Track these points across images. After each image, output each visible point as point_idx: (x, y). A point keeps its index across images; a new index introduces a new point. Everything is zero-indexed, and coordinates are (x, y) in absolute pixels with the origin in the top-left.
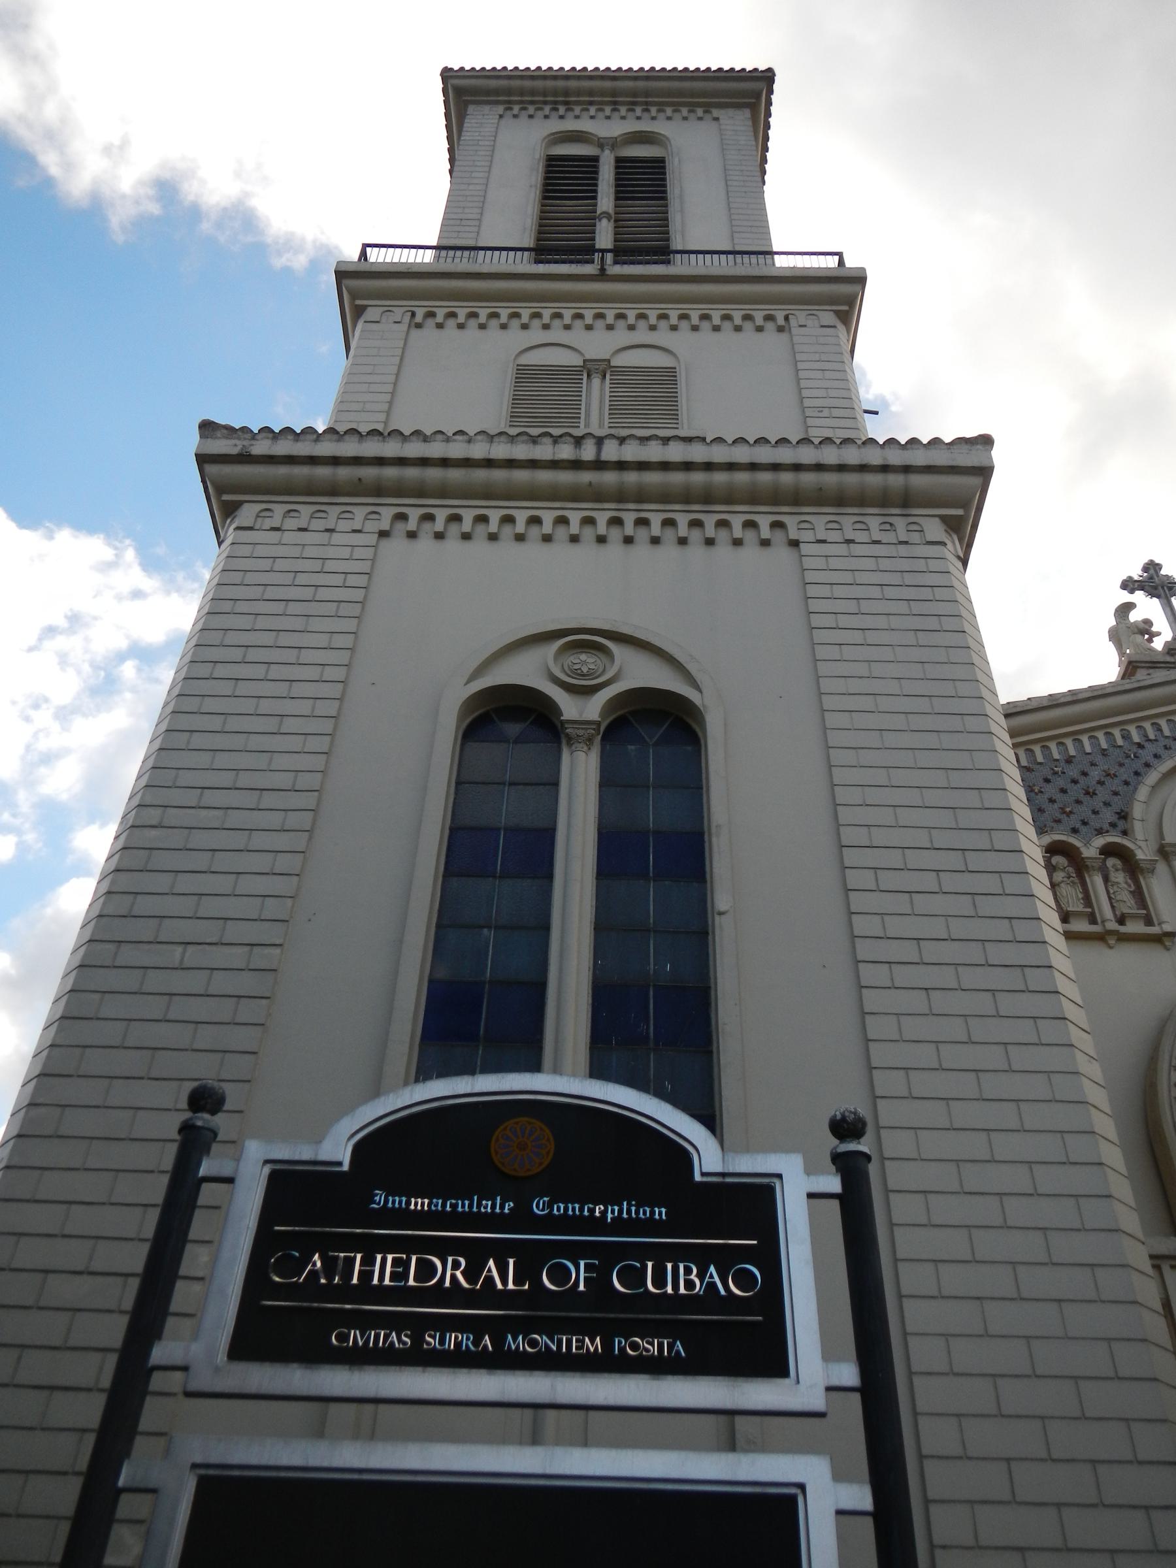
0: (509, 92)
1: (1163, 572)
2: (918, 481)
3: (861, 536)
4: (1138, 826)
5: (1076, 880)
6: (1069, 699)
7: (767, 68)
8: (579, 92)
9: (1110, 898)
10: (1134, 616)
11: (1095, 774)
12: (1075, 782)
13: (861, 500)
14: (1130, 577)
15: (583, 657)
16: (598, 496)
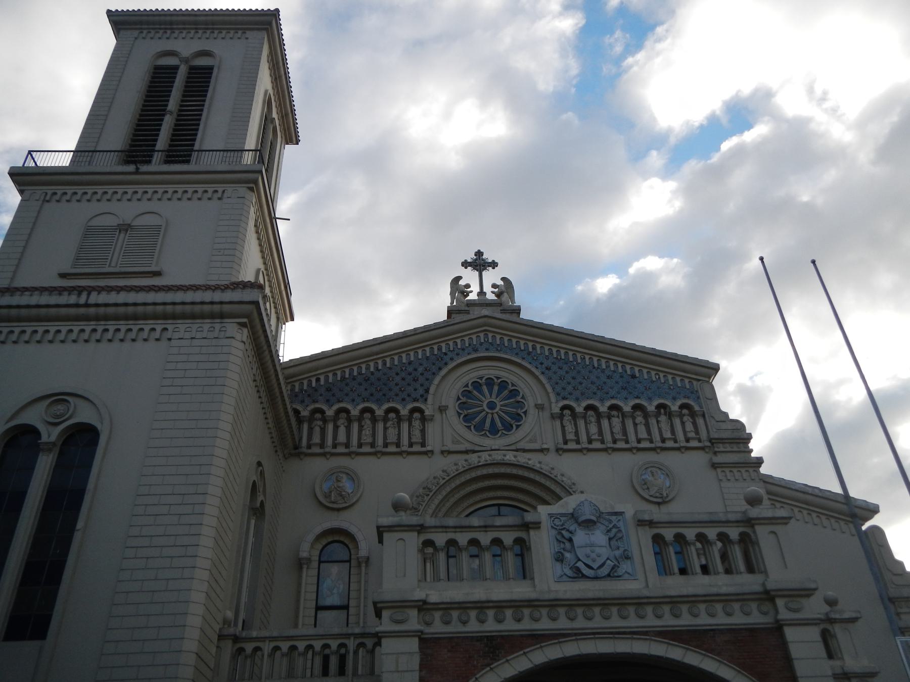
0: (141, 23)
1: (484, 257)
2: (226, 308)
3: (199, 335)
4: (430, 398)
5: (396, 425)
6: (413, 333)
7: (274, 8)
8: (178, 23)
9: (409, 433)
10: (462, 283)
11: (421, 369)
12: (410, 374)
13: (202, 316)
14: (466, 260)
15: (59, 407)
16: (87, 318)
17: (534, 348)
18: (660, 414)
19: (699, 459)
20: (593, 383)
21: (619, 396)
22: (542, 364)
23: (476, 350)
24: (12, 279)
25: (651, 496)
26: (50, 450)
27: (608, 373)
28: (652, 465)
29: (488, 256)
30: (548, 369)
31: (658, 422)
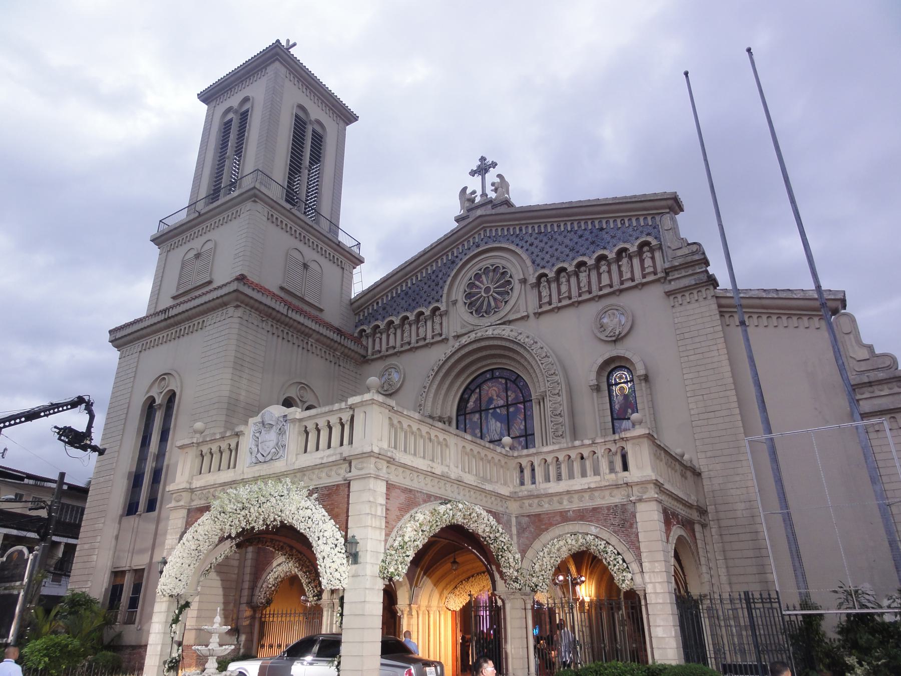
5: (424, 325)
9: (433, 328)
10: (468, 191)
17: (521, 230)
18: (623, 258)
19: (657, 291)
20: (566, 246)
21: (588, 251)
22: (527, 242)
23: (478, 246)
24: (155, 307)
25: (607, 336)
26: (159, 408)
27: (580, 233)
28: (611, 308)
29: (489, 160)
30: (531, 245)
31: (619, 267)
